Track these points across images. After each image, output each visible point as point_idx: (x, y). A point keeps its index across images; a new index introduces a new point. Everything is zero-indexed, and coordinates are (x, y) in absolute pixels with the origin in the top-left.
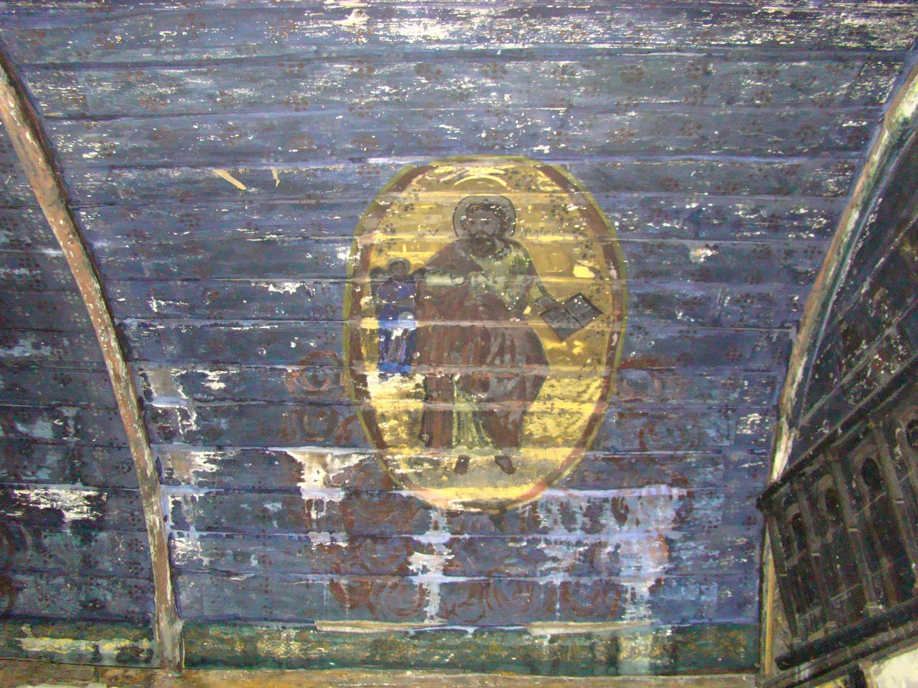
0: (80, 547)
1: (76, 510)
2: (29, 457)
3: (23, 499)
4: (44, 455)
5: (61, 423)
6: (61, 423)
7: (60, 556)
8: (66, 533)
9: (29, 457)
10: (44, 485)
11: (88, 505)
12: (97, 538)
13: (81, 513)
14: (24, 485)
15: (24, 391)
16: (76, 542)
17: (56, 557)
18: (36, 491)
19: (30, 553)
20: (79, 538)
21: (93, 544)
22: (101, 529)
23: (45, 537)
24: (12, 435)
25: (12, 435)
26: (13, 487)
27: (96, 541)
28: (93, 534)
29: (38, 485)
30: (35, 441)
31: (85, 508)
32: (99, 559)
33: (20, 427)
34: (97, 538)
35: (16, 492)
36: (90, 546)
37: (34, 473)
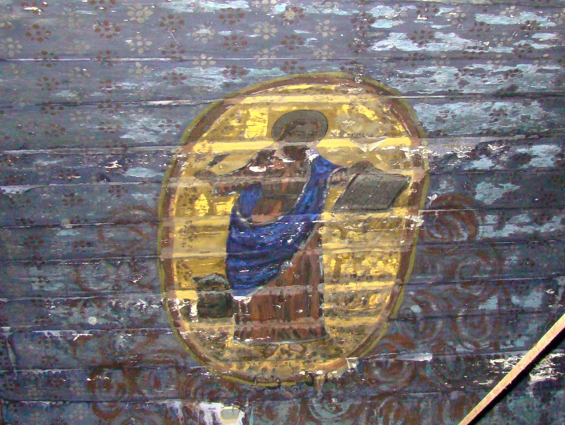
0: (540, 406)
1: (542, 372)
2: (514, 327)
3: (496, 368)
4: (527, 323)
5: (552, 292)
6: (552, 292)
7: (521, 417)
8: (529, 395)
9: (514, 327)
10: (518, 352)
11: (552, 367)
12: (555, 396)
13: (546, 374)
14: (500, 354)
15: (533, 265)
16: (536, 402)
17: (518, 418)
18: (510, 359)
19: (495, 418)
20: (540, 399)
21: (551, 402)
22: (559, 387)
23: (510, 401)
24: (504, 308)
25: (504, 308)
26: (490, 358)
27: (554, 399)
28: (552, 393)
29: (512, 353)
30: (524, 311)
31: (551, 369)
32: (555, 415)
33: (515, 300)
34: (555, 396)
35: (492, 361)
36: (549, 404)
37: (512, 342)
